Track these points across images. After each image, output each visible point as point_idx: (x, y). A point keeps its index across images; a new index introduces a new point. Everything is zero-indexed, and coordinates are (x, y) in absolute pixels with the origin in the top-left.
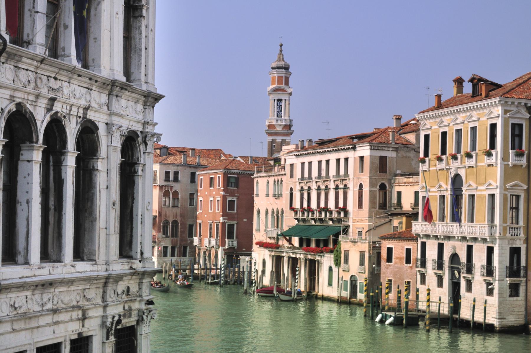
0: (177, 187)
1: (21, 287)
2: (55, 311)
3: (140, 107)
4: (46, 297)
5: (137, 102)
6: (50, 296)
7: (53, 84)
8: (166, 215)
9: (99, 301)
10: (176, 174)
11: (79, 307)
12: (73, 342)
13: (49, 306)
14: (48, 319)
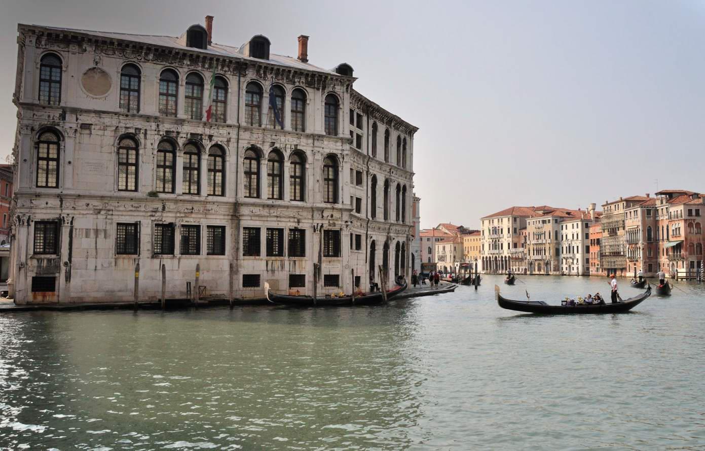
0: (698, 220)
1: (254, 205)
2: (277, 217)
3: (339, 144)
4: (272, 211)
5: (336, 142)
7: (274, 137)
8: (691, 240)
9: (310, 217)
10: (697, 211)
11: (294, 218)
14: (275, 219)
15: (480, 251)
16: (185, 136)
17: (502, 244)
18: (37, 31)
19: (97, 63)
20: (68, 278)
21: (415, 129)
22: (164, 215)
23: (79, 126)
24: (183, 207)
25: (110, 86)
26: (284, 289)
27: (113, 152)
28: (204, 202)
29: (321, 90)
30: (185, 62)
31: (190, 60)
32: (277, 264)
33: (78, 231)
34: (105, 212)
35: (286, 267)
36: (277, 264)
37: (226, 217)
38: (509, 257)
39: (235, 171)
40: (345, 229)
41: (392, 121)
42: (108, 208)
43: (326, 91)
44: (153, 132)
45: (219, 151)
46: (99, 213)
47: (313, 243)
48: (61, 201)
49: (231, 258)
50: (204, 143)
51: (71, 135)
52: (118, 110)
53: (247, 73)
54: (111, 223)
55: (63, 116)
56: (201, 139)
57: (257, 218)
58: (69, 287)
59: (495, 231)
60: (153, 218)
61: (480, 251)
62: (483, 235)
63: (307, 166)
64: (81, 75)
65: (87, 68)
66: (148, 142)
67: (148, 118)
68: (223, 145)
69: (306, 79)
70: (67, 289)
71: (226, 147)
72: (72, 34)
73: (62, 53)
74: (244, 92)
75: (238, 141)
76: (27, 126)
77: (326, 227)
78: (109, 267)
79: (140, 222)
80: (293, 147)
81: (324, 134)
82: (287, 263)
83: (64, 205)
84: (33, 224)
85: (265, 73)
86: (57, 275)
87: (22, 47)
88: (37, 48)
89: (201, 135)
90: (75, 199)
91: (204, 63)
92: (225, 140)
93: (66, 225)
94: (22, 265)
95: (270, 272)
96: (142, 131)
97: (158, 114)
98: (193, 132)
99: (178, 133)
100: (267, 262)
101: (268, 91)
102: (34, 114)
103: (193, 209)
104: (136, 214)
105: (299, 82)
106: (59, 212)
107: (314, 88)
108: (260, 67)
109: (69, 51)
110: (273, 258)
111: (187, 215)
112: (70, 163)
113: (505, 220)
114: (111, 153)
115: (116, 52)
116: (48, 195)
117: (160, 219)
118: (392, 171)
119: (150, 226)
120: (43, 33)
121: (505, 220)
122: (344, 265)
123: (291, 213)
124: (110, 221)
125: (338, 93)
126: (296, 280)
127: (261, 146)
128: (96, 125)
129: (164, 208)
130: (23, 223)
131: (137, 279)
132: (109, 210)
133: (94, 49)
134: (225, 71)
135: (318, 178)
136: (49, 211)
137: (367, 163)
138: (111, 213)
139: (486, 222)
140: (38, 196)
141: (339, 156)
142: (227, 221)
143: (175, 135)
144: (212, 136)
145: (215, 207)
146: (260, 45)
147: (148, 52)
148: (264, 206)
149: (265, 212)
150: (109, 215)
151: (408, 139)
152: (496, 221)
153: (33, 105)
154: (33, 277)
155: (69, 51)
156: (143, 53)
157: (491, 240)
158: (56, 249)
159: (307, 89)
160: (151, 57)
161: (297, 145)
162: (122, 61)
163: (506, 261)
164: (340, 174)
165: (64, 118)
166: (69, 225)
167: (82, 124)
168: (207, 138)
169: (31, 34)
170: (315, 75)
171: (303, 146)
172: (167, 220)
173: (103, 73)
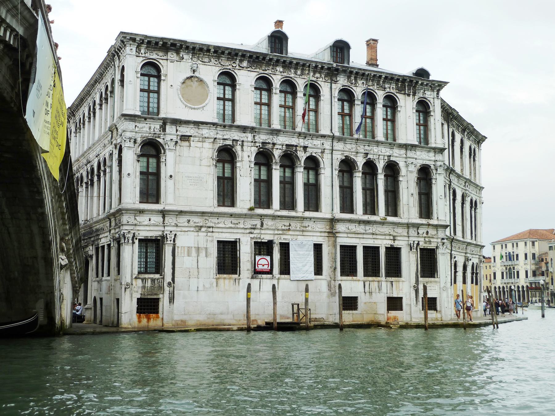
1: (350, 221)
4: (367, 228)
5: (429, 151)
6: (371, 227)
7: (367, 147)
9: (406, 234)
11: (390, 235)
12: (386, 248)
13: (371, 231)
14: (371, 236)
15: (490, 280)
16: (280, 147)
17: (518, 272)
18: (138, 39)
19: (194, 71)
20: (172, 299)
21: (484, 138)
22: (263, 232)
23: (179, 137)
24: (280, 224)
25: (207, 96)
26: (382, 313)
27: (212, 165)
28: (301, 217)
29: (411, 96)
30: (278, 68)
31: (283, 67)
32: (374, 285)
33: (180, 249)
34: (206, 229)
35: (383, 287)
36: (374, 285)
37: (323, 234)
38: (527, 286)
39: (330, 184)
40: (441, 247)
41: (467, 129)
42: (208, 225)
43: (416, 97)
44: (250, 144)
45: (313, 164)
46: (200, 229)
47: (410, 262)
48: (164, 217)
49: (329, 279)
50: (299, 155)
51: (172, 148)
52: (216, 121)
53: (338, 79)
54: (212, 241)
55: (163, 128)
56: (296, 151)
57: (353, 236)
58: (173, 309)
59: (510, 257)
60: (252, 236)
61: (490, 280)
62: (495, 261)
63: (401, 179)
64: (180, 84)
65: (185, 77)
66: (245, 154)
67: (245, 128)
68: (318, 156)
69: (397, 84)
70: (171, 312)
71: (320, 159)
72: (171, 41)
73: (161, 61)
74: (336, 100)
75: (332, 154)
76: (130, 139)
77: (422, 245)
78: (210, 288)
79: (239, 239)
80: (386, 158)
81: (417, 143)
82: (384, 284)
83: (166, 222)
84: (137, 242)
85: (356, 79)
86: (161, 296)
87: (114, 56)
88: (137, 56)
89: (296, 146)
90: (177, 215)
91: (296, 69)
92: (320, 151)
93: (169, 242)
94: (127, 285)
95: (368, 294)
96: (239, 143)
97: (254, 125)
98: (287, 143)
99: (274, 144)
100: (364, 283)
101: (360, 98)
102: (136, 126)
103: (290, 225)
104: (235, 231)
105: (390, 88)
106: (162, 229)
107: (405, 94)
108: (351, 72)
109: (167, 60)
110: (370, 279)
111: (285, 232)
112: (171, 176)
113: (521, 244)
114: (210, 166)
115: (212, 59)
116: (152, 211)
117: (259, 236)
118: (467, 184)
119: (249, 243)
120: (143, 40)
121: (521, 244)
122: (442, 286)
123: (386, 229)
124: (210, 239)
125: (429, 99)
126: (394, 303)
127: (354, 158)
128: (195, 137)
129: (262, 225)
130: (128, 241)
131: (248, 300)
132: (209, 227)
133: (191, 57)
134: (317, 78)
135: (412, 192)
136: (152, 228)
137: (449, 176)
138: (211, 230)
139: (498, 247)
140: (142, 212)
141: (432, 167)
142: (323, 239)
143: (270, 146)
144: (307, 147)
145: (311, 224)
146: (341, 48)
147: (242, 58)
148: (360, 222)
149: (361, 228)
150: (209, 232)
151: (477, 150)
152: (510, 246)
153: (135, 116)
154: (138, 299)
155: (167, 60)
156: (238, 61)
157: (504, 268)
158: (159, 268)
159: (397, 95)
160: (245, 64)
161: (390, 156)
162: (218, 69)
163: (523, 291)
164: (434, 187)
165: (164, 130)
166: (172, 242)
167: (182, 136)
168: (302, 148)
169: (131, 42)
170: (406, 80)
171: (396, 157)
172: (266, 238)
173: (201, 81)
